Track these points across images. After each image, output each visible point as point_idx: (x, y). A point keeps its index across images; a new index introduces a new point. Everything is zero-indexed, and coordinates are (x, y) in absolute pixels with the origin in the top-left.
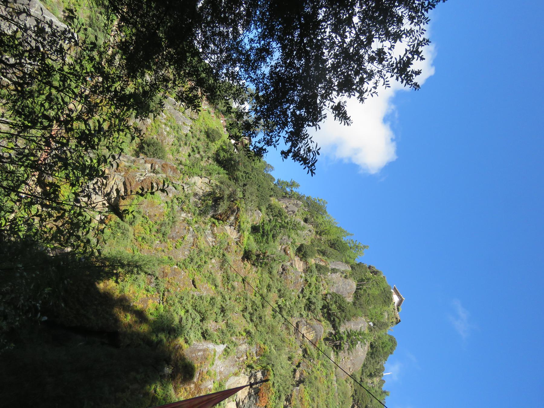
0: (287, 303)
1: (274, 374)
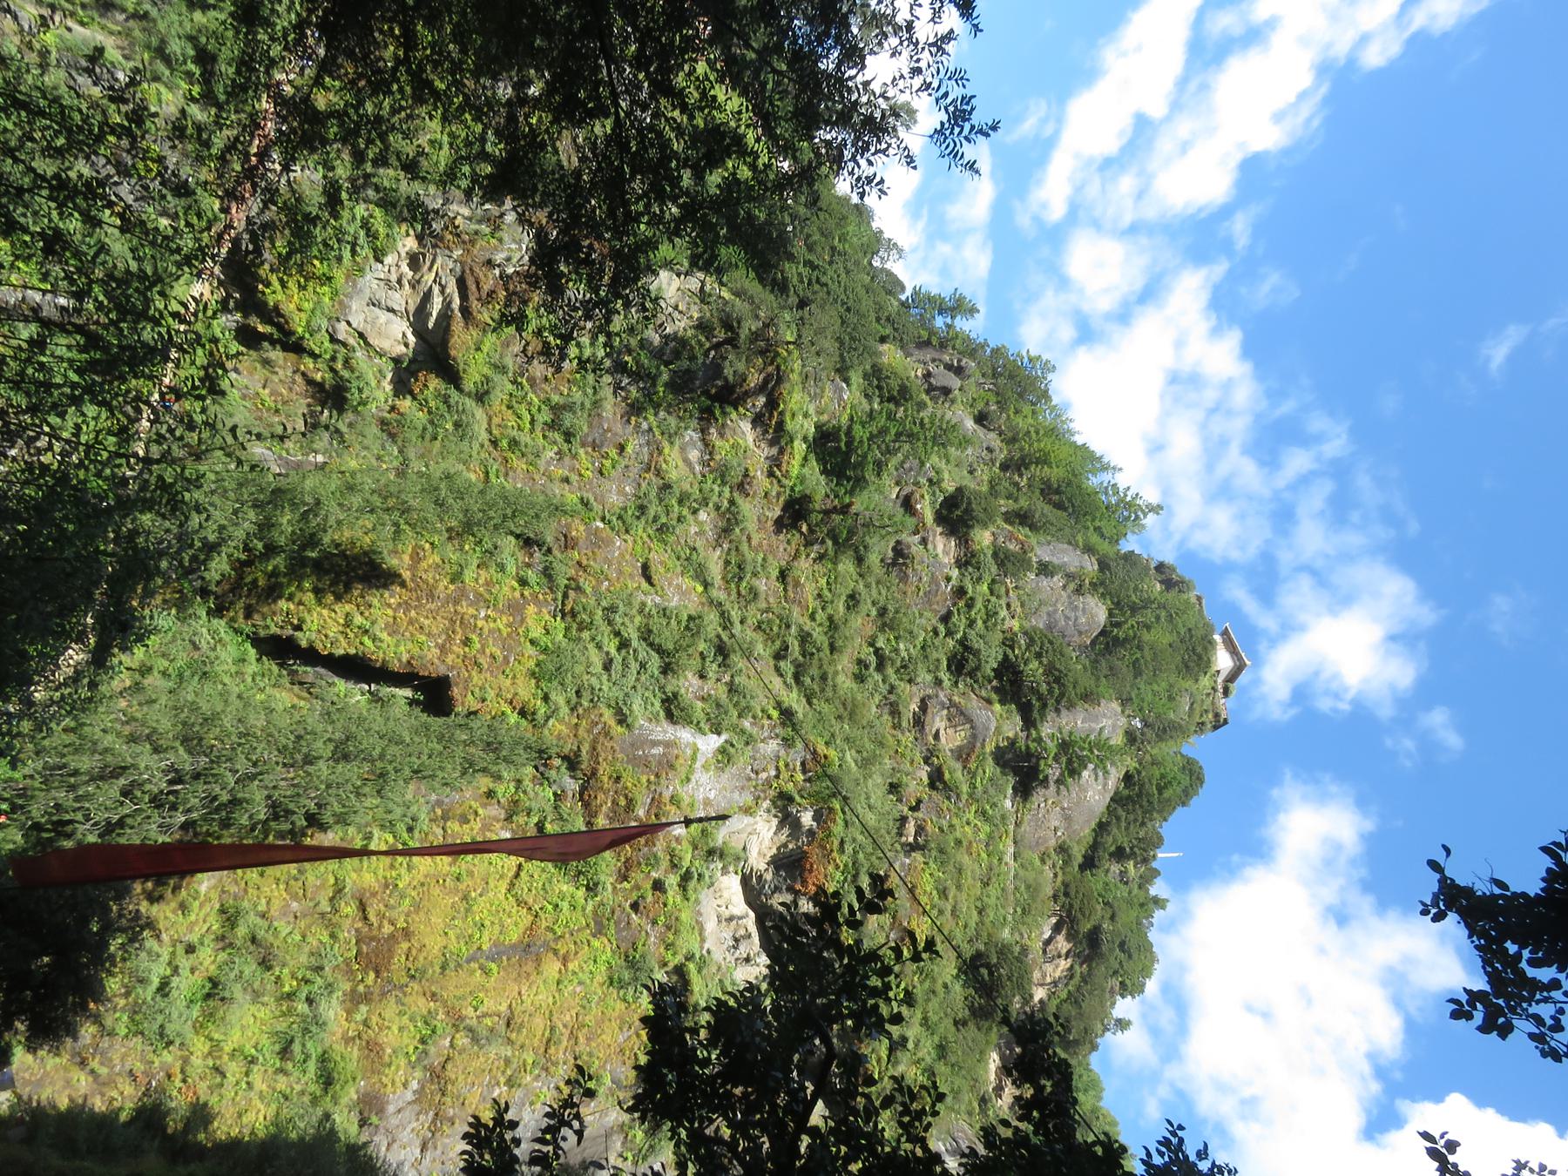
0: (902, 646)
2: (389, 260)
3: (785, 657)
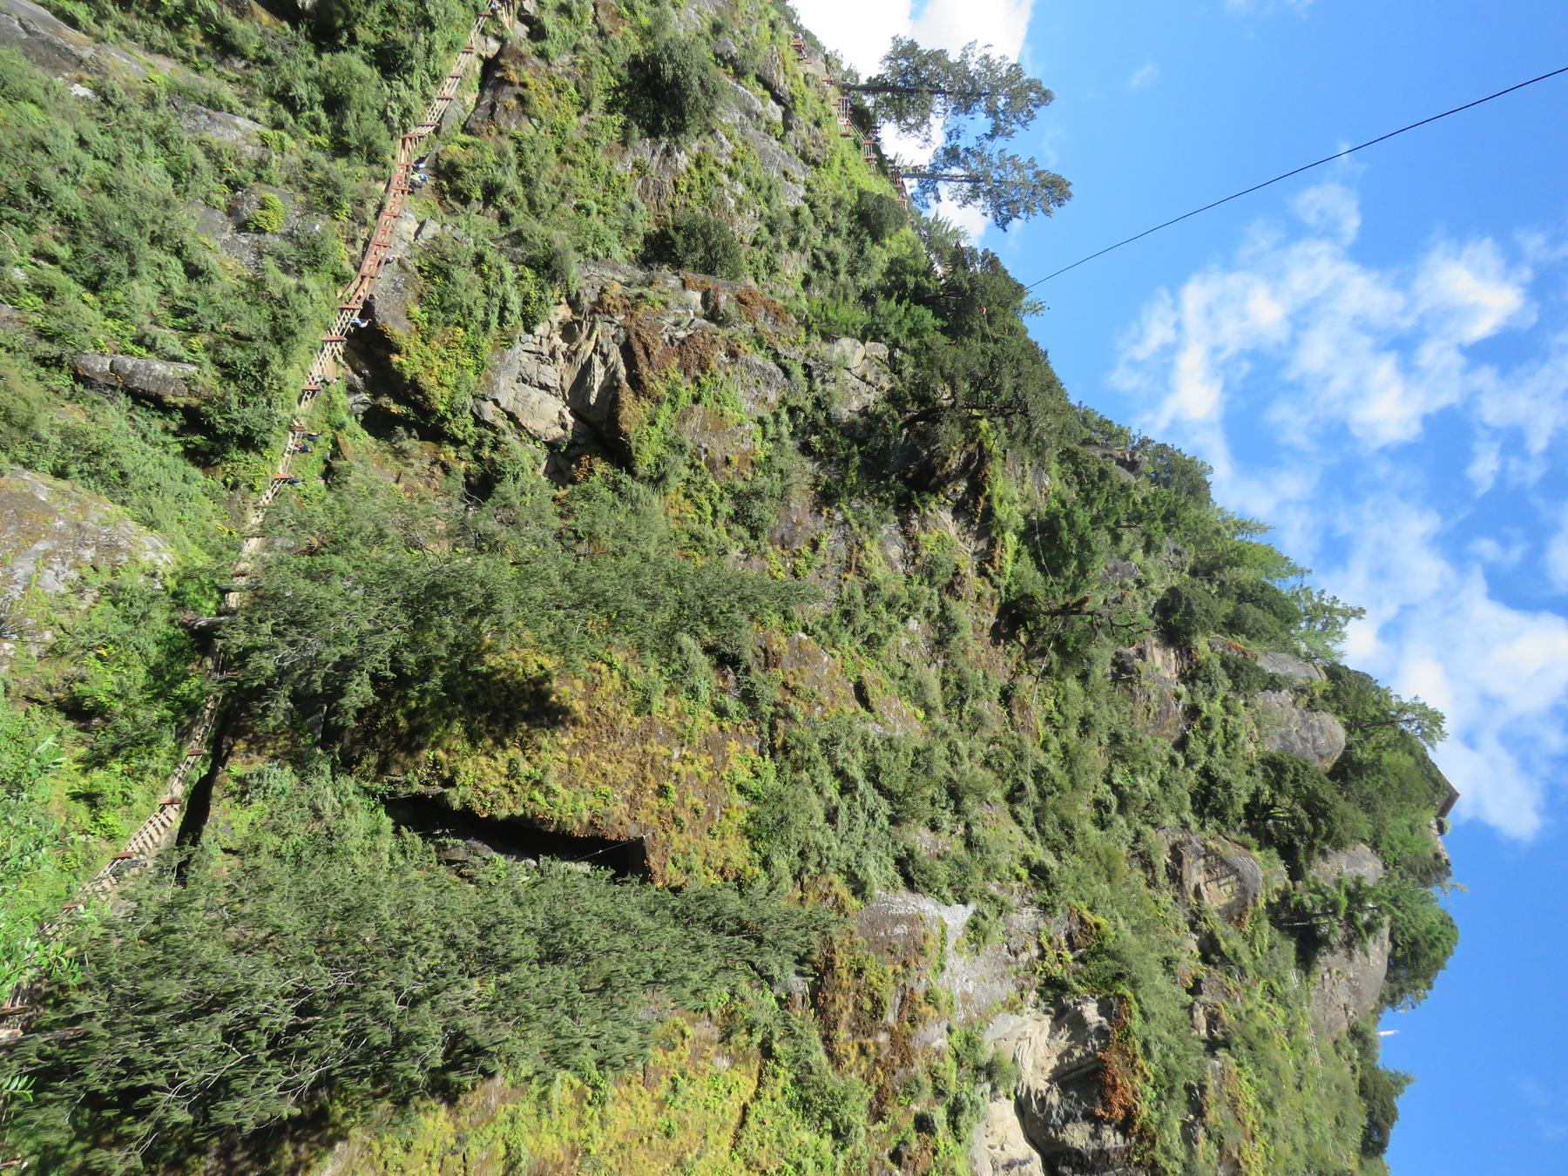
0: (1141, 780)
1: (1142, 1012)
2: (540, 329)
3: (1020, 800)
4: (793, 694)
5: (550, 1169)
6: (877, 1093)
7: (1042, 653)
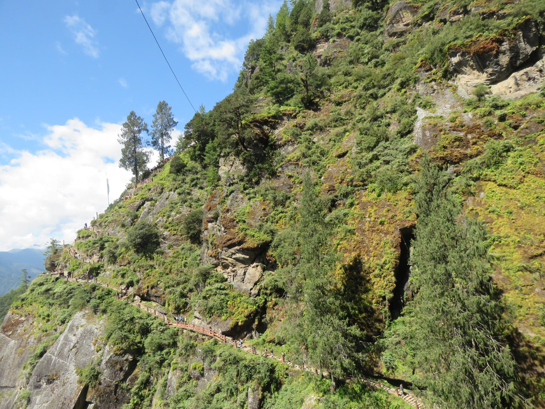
0: (366, 51)
1: (454, 40)
2: (226, 276)
3: (376, 95)
4: (343, 180)
5: (526, 255)
6: (491, 137)
7: (322, 92)
